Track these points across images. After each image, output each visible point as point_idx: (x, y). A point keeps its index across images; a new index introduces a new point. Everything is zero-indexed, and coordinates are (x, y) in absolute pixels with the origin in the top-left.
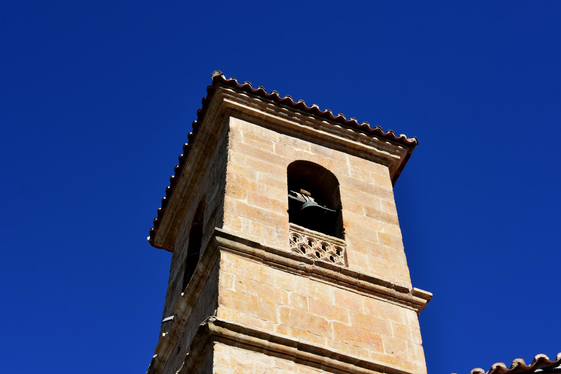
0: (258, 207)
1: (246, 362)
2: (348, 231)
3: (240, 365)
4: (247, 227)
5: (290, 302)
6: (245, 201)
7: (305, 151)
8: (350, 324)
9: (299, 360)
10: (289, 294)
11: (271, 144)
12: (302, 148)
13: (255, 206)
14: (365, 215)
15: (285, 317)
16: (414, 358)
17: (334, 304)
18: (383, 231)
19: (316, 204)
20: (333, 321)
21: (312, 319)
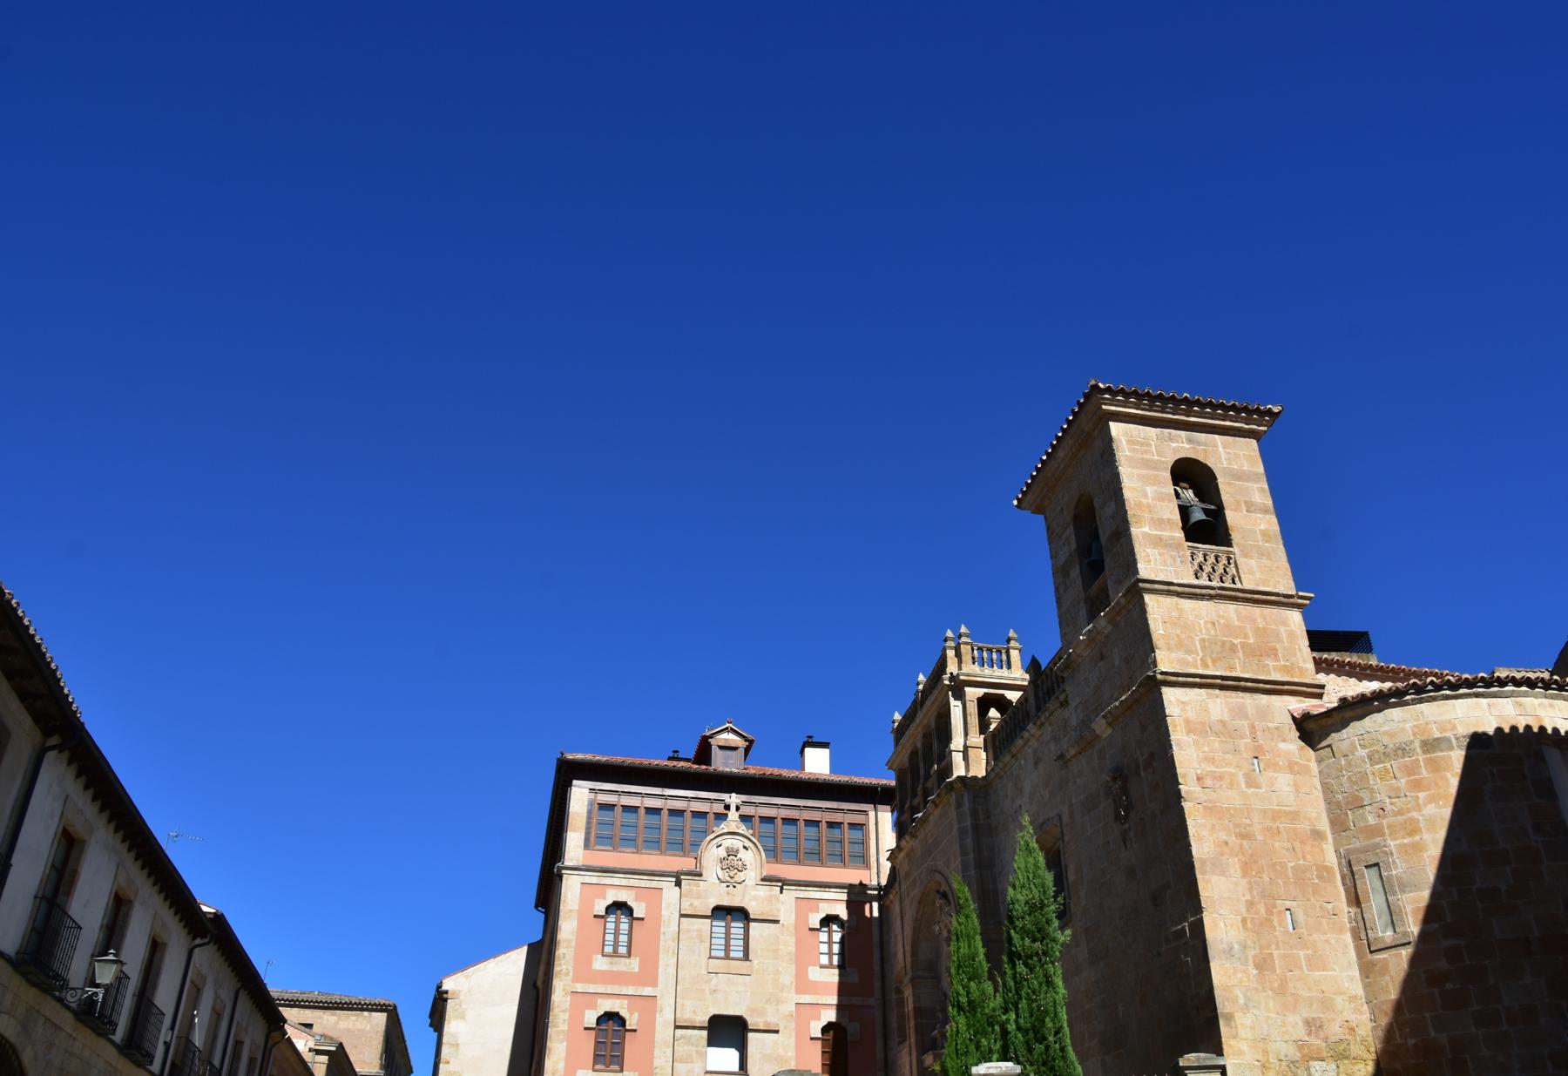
0: (1159, 533)
1: (1186, 699)
2: (1235, 536)
3: (1183, 702)
4: (1156, 559)
5: (1204, 631)
6: (1146, 529)
7: (1181, 445)
8: (1252, 641)
9: (1222, 688)
10: (1202, 622)
11: (1150, 445)
12: (1178, 442)
13: (1156, 533)
14: (1245, 512)
15: (1203, 648)
16: (1305, 662)
17: (1237, 623)
18: (1262, 527)
19: (1204, 518)
20: (1239, 640)
21: (1224, 643)
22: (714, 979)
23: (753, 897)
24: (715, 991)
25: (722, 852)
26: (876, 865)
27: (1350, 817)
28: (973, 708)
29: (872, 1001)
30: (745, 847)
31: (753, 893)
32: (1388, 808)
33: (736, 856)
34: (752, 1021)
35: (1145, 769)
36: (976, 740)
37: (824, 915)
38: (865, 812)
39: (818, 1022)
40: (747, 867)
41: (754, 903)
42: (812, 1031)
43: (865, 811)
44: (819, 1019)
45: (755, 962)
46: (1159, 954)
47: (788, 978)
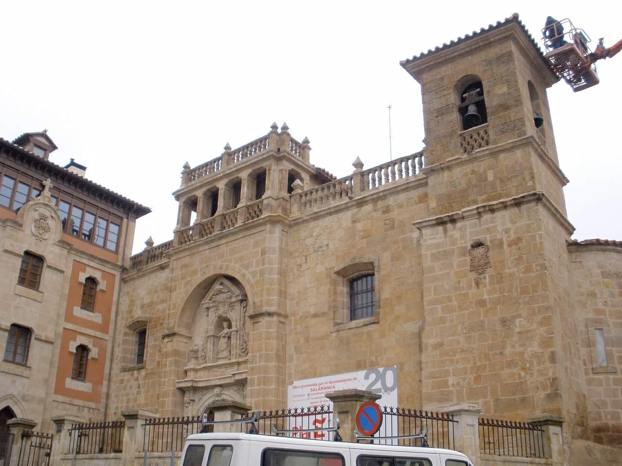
22: (18, 300)
23: (51, 252)
24: (17, 307)
25: (36, 215)
26: (122, 253)
27: (589, 302)
28: (286, 176)
29: (106, 337)
30: (52, 217)
31: (52, 249)
32: (609, 302)
33: (45, 220)
34: (37, 332)
35: (510, 245)
36: (286, 195)
37: (88, 276)
38: (122, 218)
39: (74, 342)
40: (51, 230)
41: (50, 256)
42: (70, 347)
43: (122, 218)
44: (75, 340)
45: (46, 294)
46: (501, 353)
47: (63, 311)
